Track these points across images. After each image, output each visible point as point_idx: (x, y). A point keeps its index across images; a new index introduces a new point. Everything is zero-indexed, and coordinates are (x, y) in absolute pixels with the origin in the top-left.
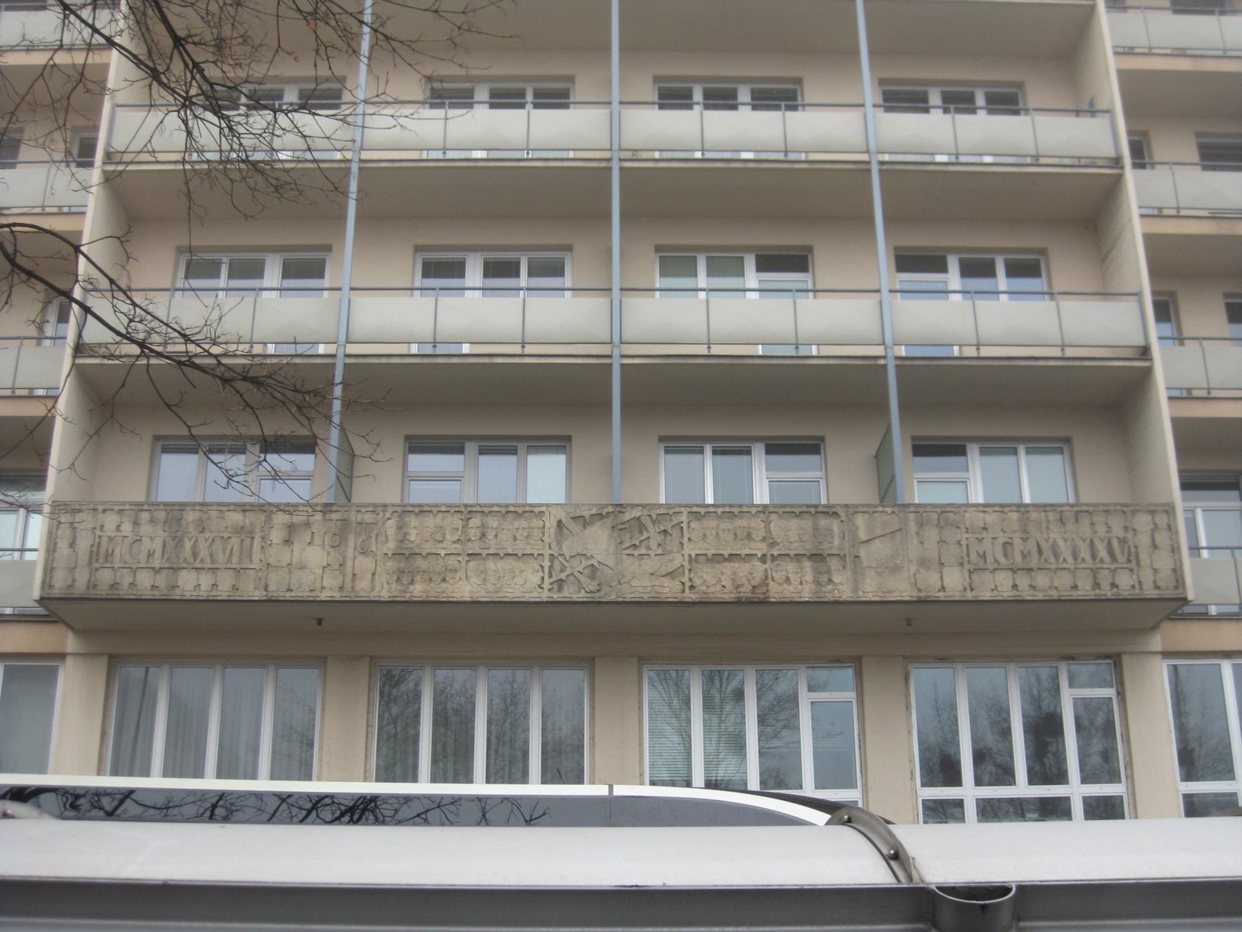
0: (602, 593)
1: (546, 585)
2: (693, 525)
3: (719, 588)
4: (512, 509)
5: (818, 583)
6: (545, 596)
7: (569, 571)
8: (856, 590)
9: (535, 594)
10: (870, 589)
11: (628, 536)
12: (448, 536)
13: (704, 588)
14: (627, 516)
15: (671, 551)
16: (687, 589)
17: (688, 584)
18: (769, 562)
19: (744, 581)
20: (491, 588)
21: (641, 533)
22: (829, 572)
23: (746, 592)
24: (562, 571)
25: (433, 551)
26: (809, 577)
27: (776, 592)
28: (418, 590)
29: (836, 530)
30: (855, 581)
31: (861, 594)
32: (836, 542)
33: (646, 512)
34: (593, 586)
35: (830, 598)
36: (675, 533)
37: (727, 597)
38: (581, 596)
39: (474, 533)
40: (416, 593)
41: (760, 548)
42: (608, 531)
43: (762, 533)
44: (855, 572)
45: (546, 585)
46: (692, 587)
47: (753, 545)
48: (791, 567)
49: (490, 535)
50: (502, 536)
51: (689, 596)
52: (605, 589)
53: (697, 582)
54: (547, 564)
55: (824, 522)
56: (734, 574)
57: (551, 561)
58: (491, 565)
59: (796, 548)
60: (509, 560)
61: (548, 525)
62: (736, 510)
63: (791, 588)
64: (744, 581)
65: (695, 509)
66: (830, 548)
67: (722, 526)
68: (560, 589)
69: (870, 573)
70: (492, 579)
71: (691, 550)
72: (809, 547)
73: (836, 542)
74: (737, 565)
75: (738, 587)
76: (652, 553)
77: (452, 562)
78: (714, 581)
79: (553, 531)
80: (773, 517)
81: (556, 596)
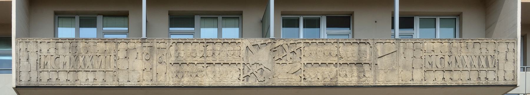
0: (266, 82)
1: (241, 78)
2: (306, 48)
3: (316, 79)
4: (226, 41)
5: (359, 77)
6: (241, 83)
7: (251, 71)
8: (375, 80)
9: (237, 83)
10: (381, 80)
11: (277, 55)
12: (198, 54)
13: (310, 79)
14: (277, 45)
15: (296, 62)
16: (302, 80)
17: (303, 77)
18: (338, 67)
19: (327, 76)
20: (218, 80)
21: (283, 52)
22: (364, 71)
23: (328, 82)
24: (248, 72)
25: (191, 62)
26: (355, 74)
27: (342, 81)
28: (186, 81)
29: (368, 51)
30: (375, 76)
31: (377, 82)
32: (368, 58)
33: (285, 42)
34: (262, 80)
35: (363, 84)
36: (298, 52)
37: (320, 84)
38: (257, 84)
39: (209, 53)
40: (185, 82)
41: (335, 60)
42: (269, 51)
43: (336, 53)
44: (375, 71)
45: (241, 78)
46: (304, 79)
47: (332, 58)
48: (347, 69)
49: (217, 53)
50: (221, 54)
51: (303, 83)
52: (267, 80)
53: (307, 76)
54: (241, 68)
55: (363, 47)
56: (323, 72)
57: (244, 67)
58: (218, 68)
59: (352, 60)
60: (225, 66)
61: (242, 49)
62: (325, 42)
63: (347, 79)
64: (327, 76)
65: (307, 41)
66: (365, 60)
67: (319, 49)
68: (247, 81)
69: (382, 72)
70: (218, 75)
71: (305, 61)
72: (354, 60)
73: (368, 58)
74: (324, 68)
75: (324, 79)
76: (288, 63)
77: (200, 67)
78: (314, 76)
79: (244, 52)
80: (341, 45)
81: (246, 84)
